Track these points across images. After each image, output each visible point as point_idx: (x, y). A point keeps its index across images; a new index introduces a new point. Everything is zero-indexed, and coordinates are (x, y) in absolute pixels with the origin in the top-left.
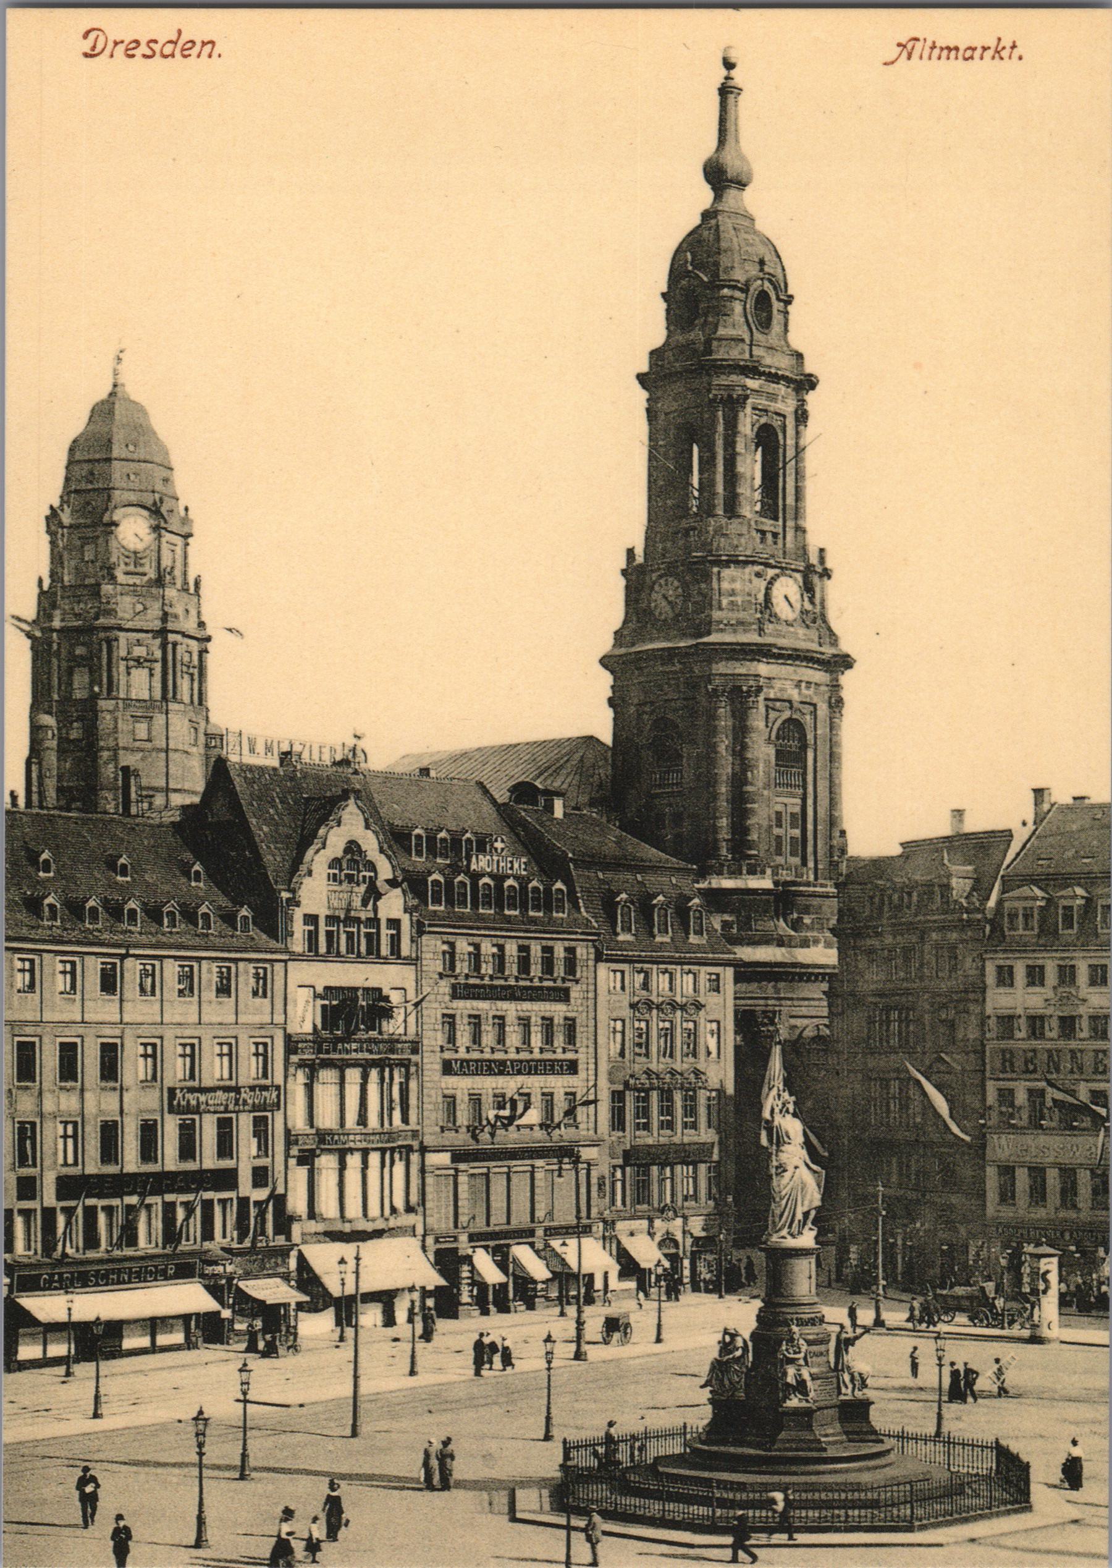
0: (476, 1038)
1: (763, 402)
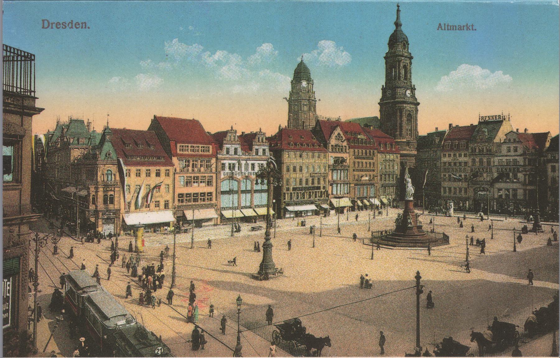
0: (359, 166)
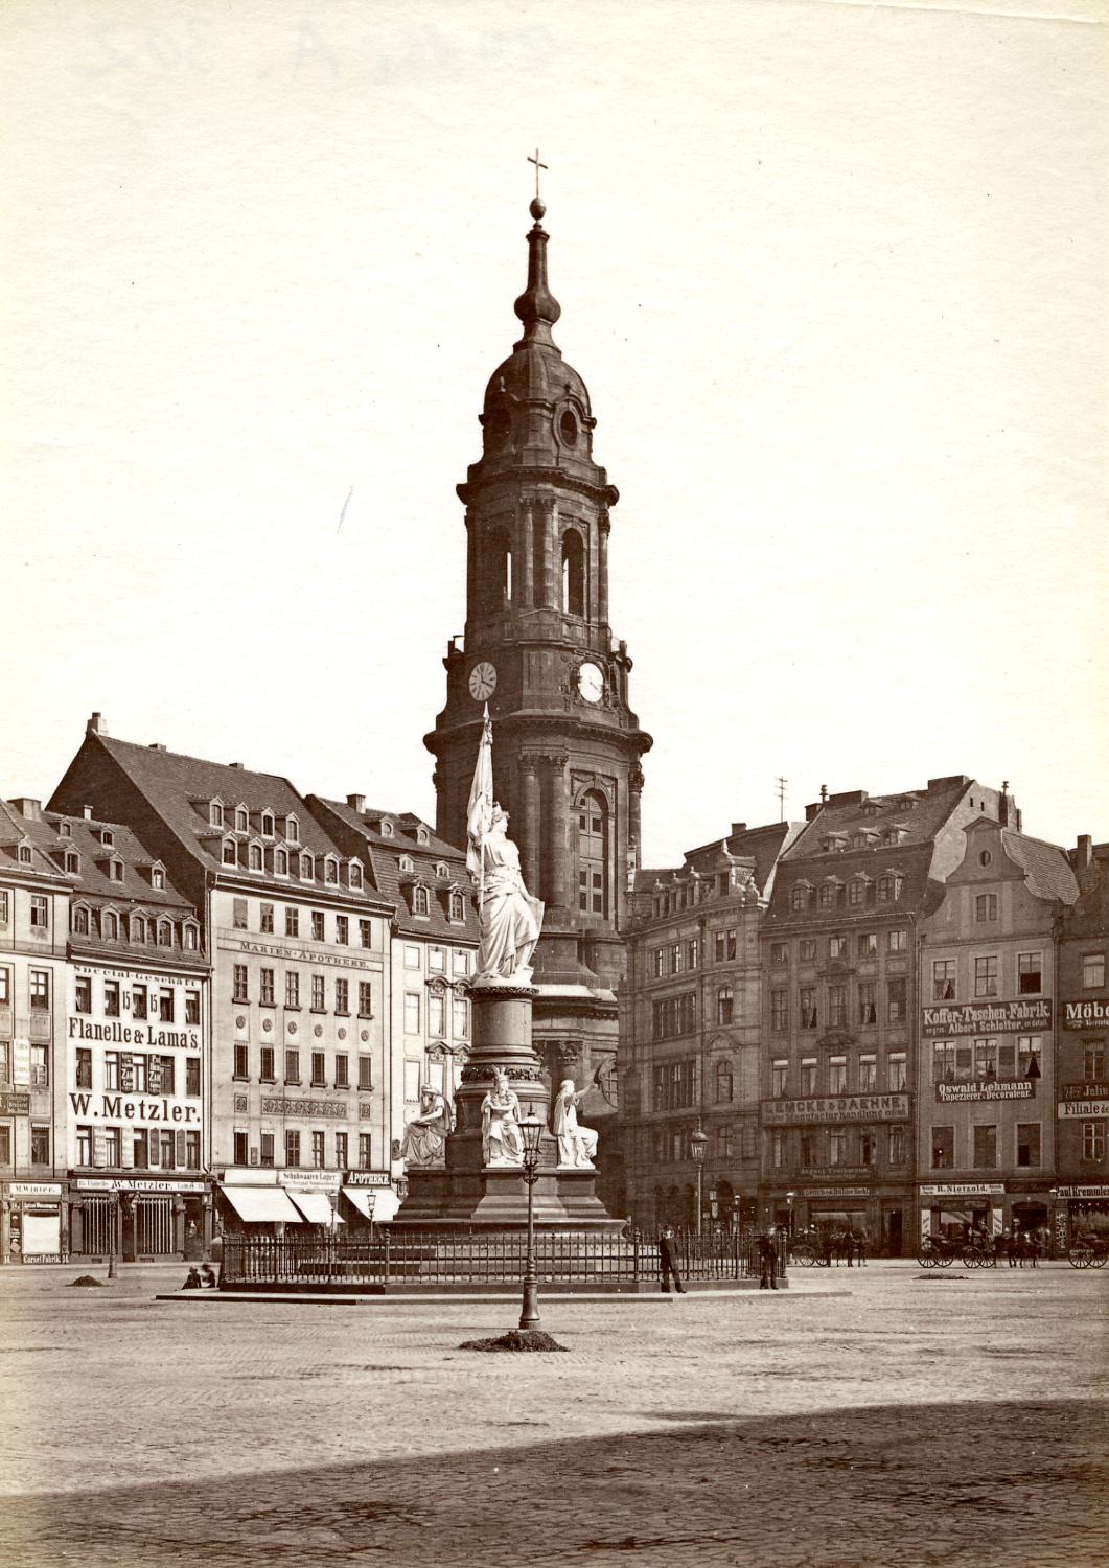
1: (568, 507)
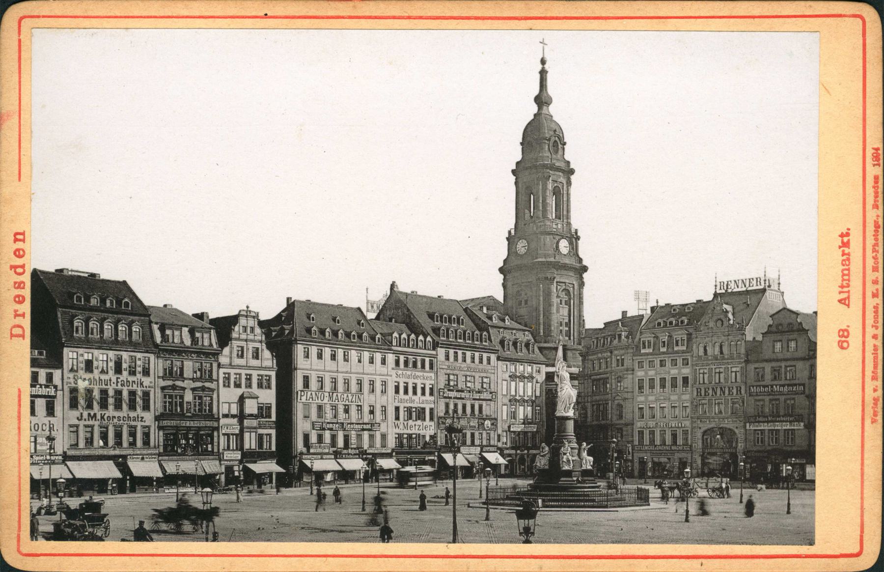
1: (555, 178)
